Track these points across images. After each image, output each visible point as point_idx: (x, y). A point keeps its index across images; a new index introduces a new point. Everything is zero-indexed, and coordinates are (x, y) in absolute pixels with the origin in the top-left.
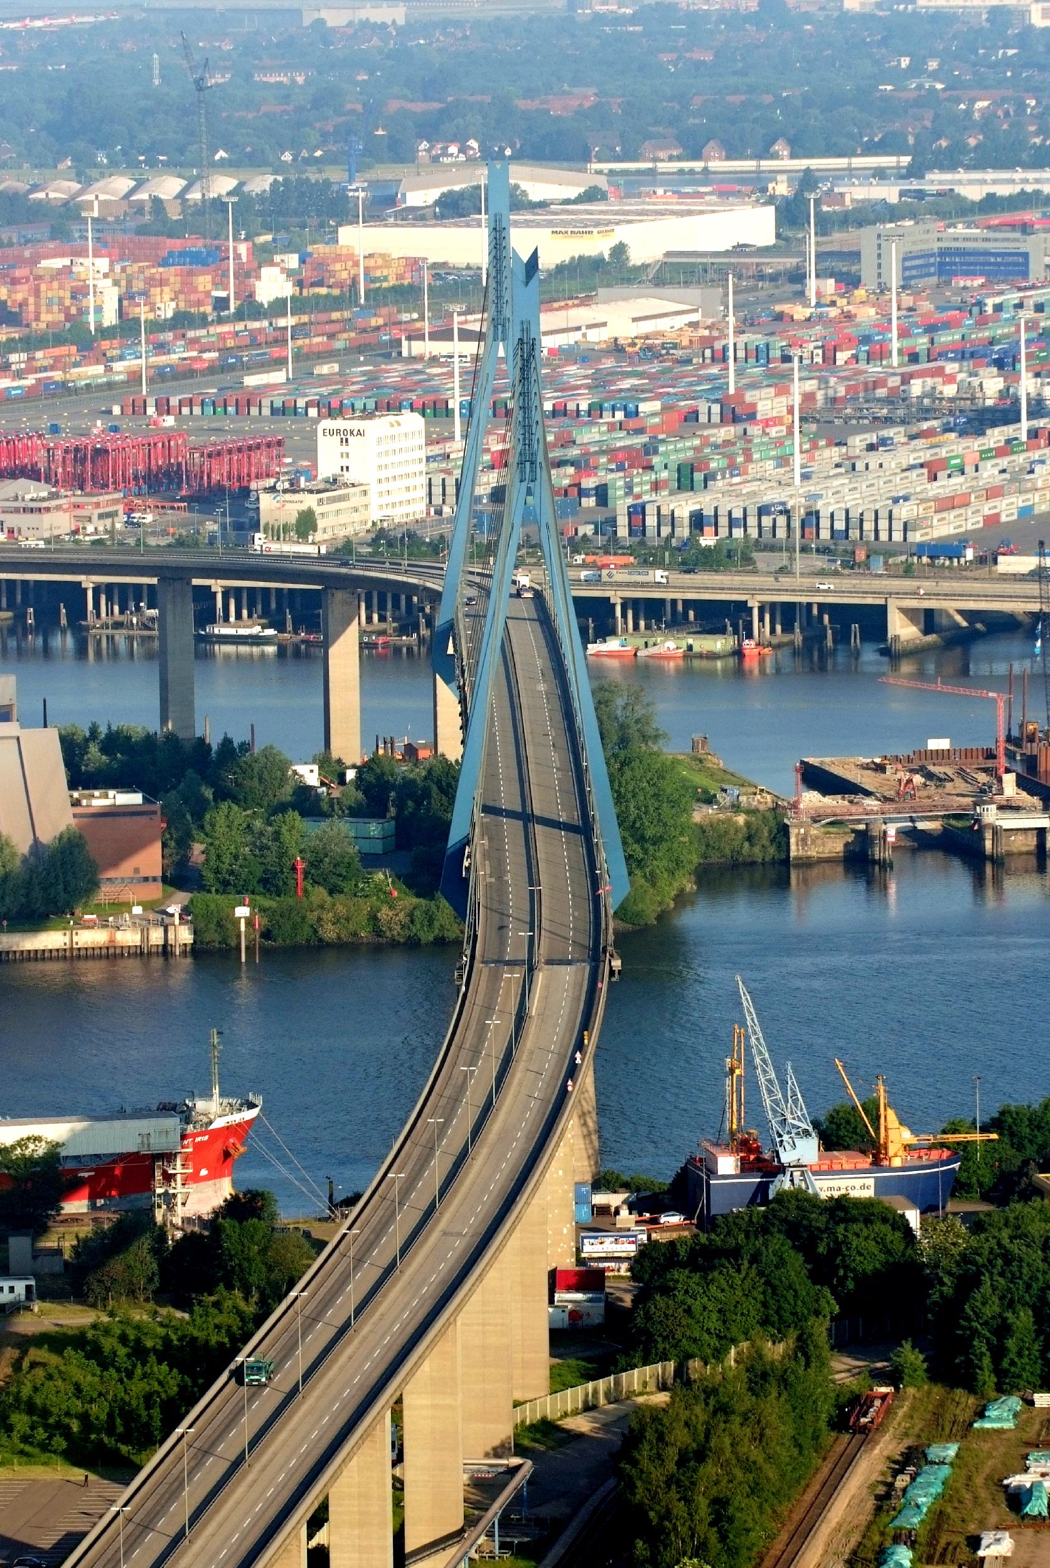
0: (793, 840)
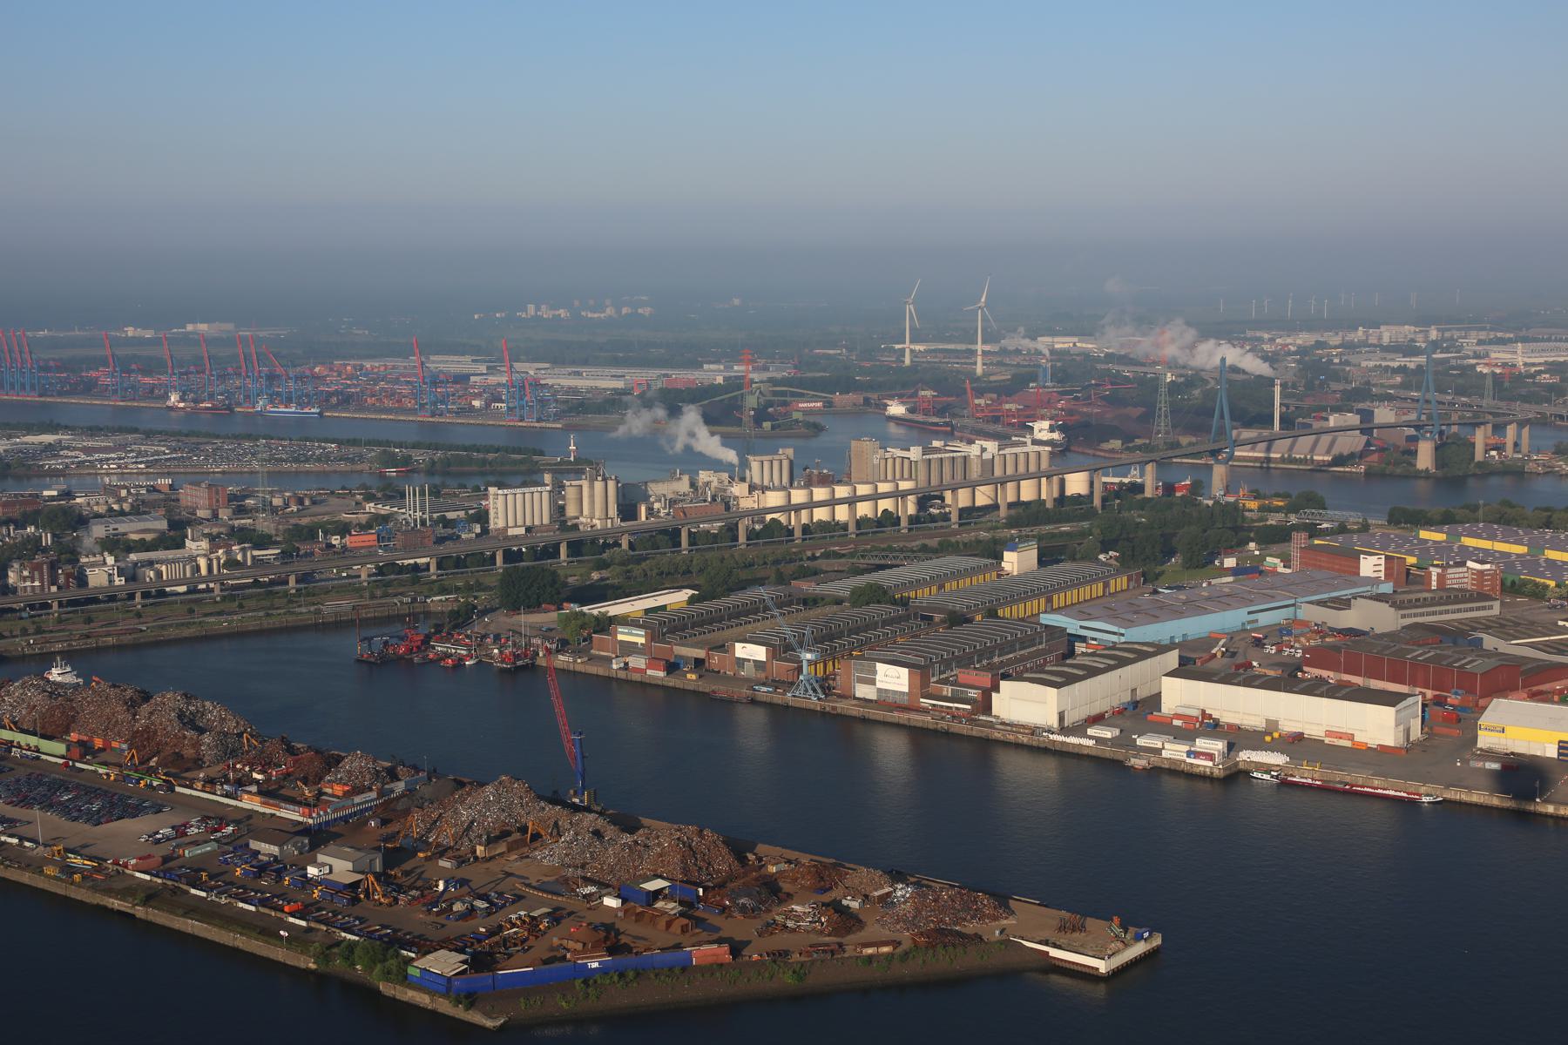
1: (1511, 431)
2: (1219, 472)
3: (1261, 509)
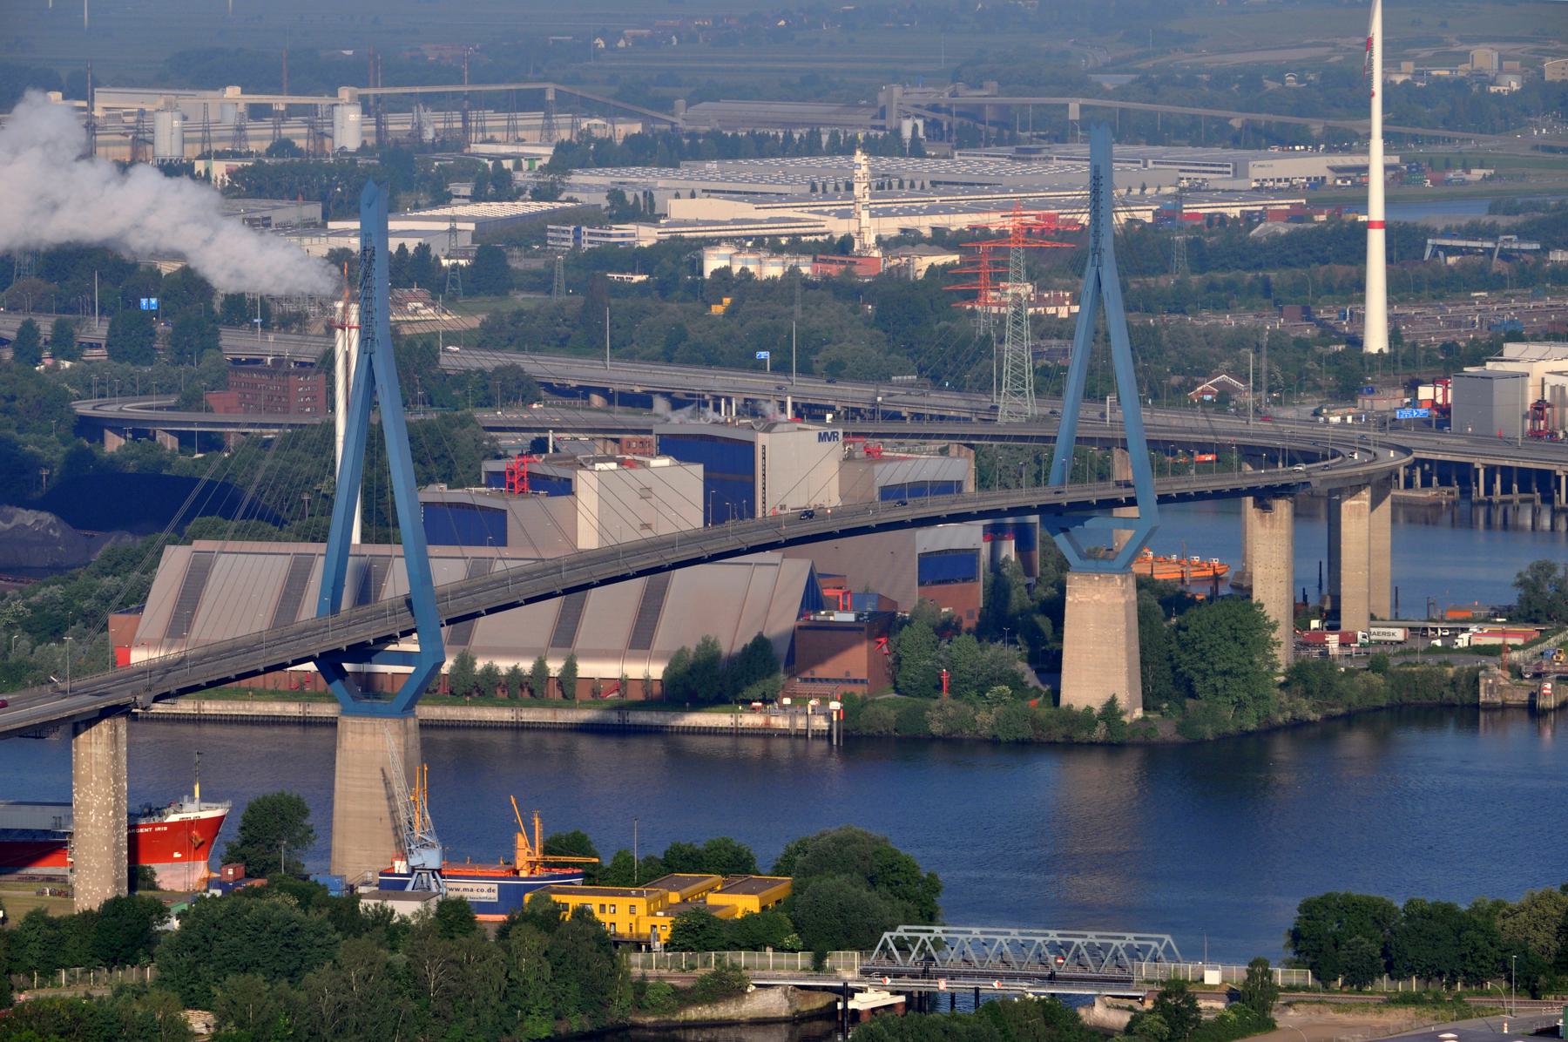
0: (1482, 688)
1: (1363, 527)
2: (372, 756)
3: (696, 932)
